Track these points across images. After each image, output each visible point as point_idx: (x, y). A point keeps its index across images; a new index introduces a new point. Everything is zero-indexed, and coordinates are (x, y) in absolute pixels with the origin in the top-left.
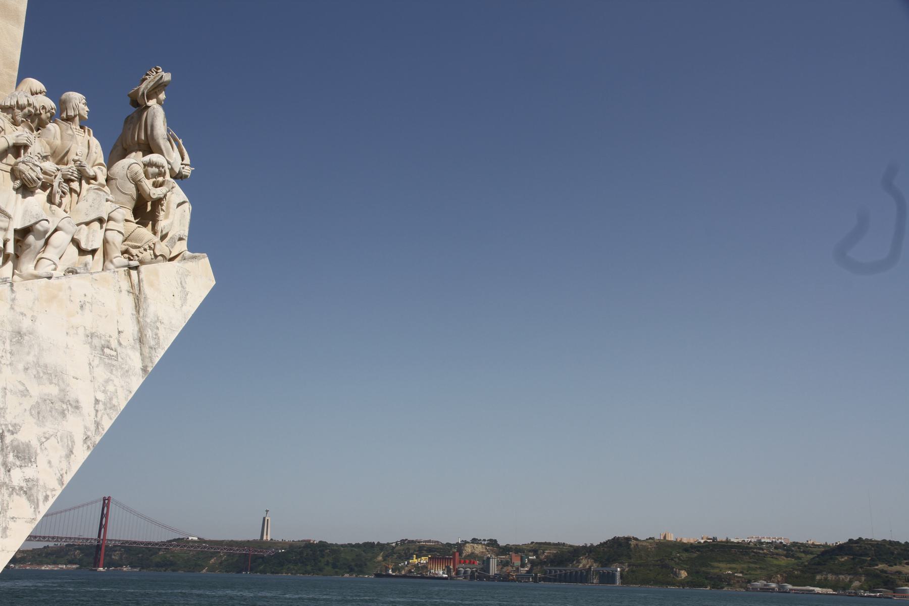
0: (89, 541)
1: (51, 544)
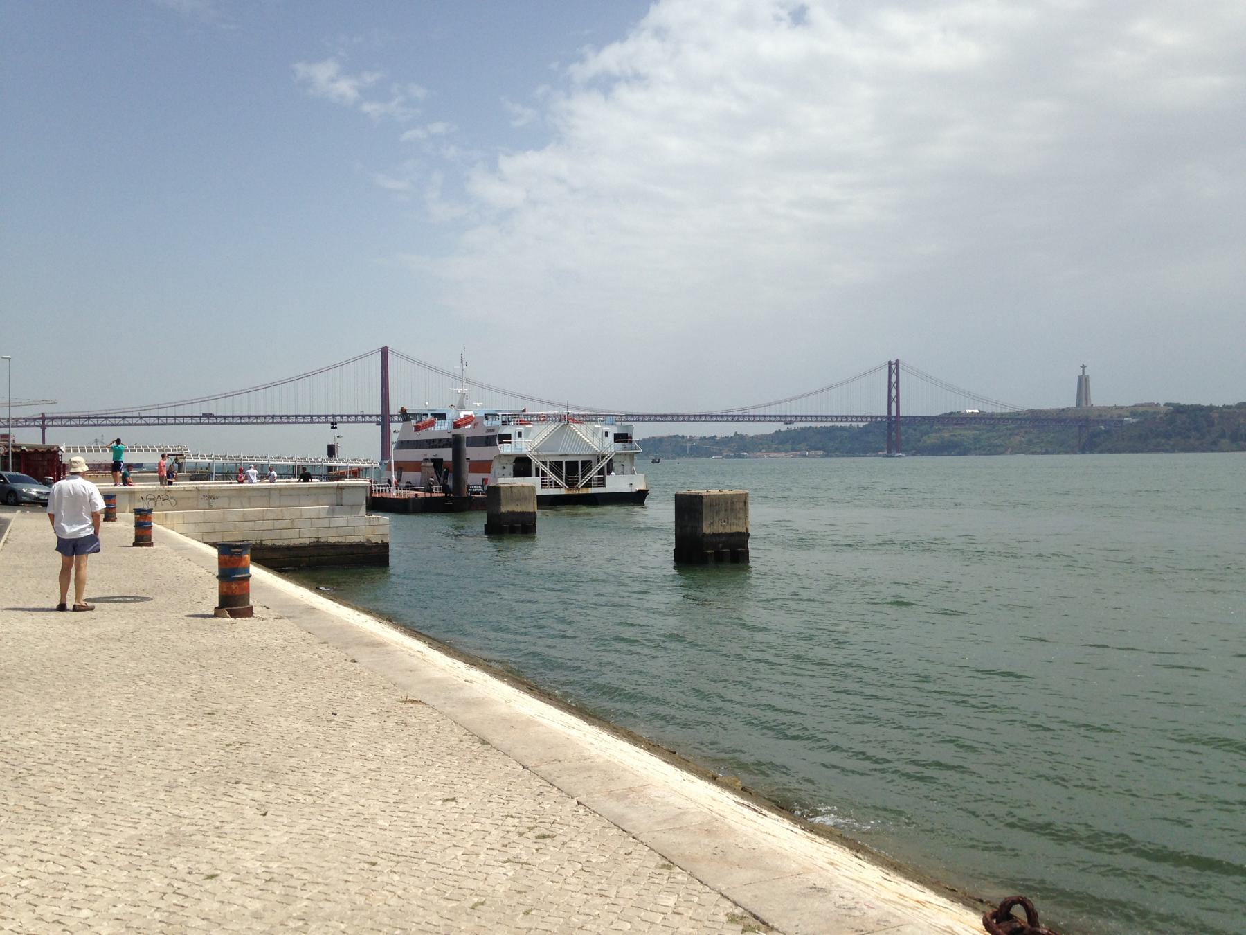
1: (782, 427)
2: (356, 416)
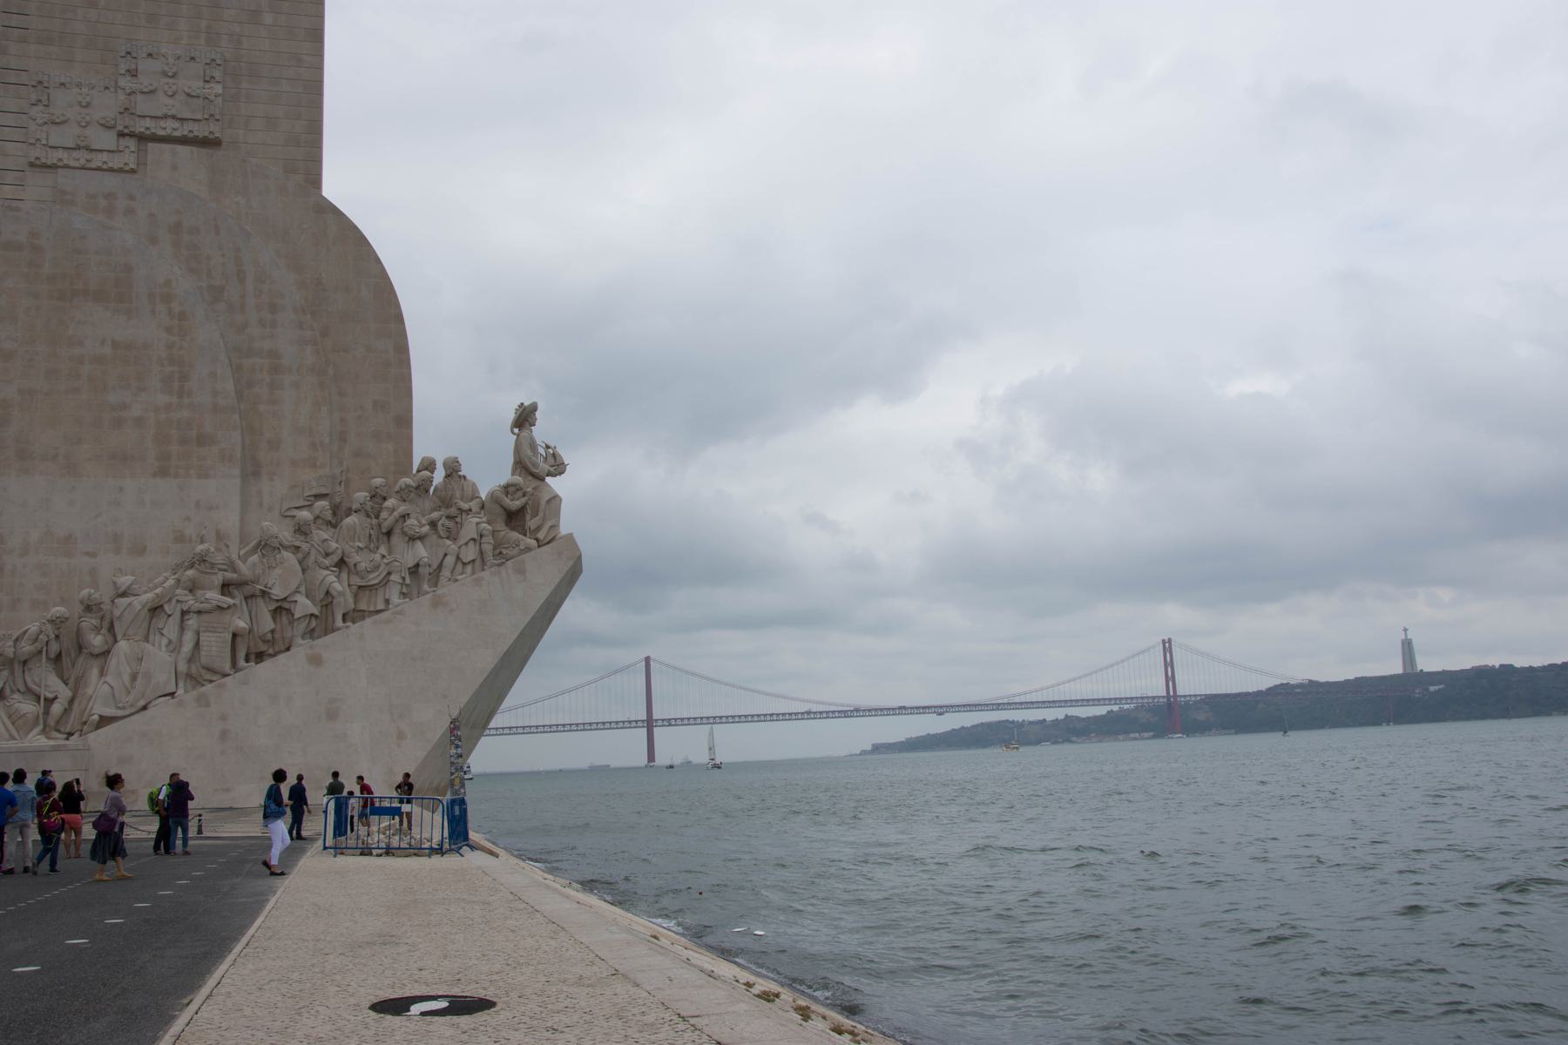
0: (1156, 700)
1: (1115, 708)
2: (623, 722)
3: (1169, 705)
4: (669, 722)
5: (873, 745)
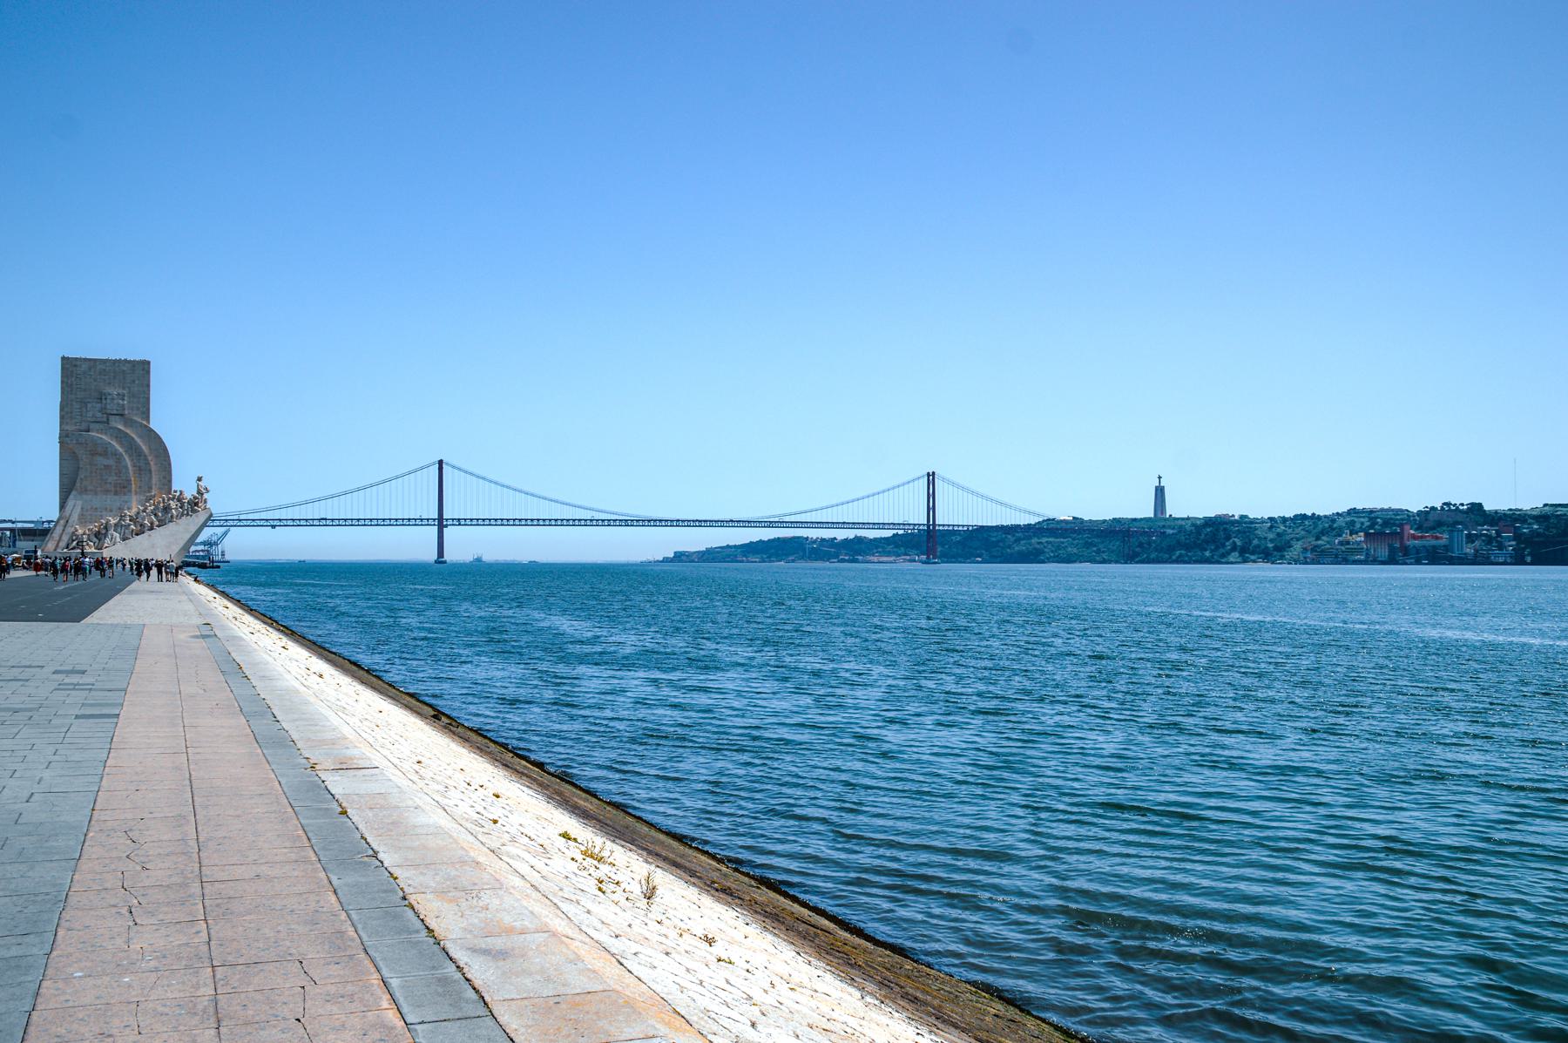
1: (901, 532)
3: (928, 531)
4: (459, 522)
5: (675, 553)
